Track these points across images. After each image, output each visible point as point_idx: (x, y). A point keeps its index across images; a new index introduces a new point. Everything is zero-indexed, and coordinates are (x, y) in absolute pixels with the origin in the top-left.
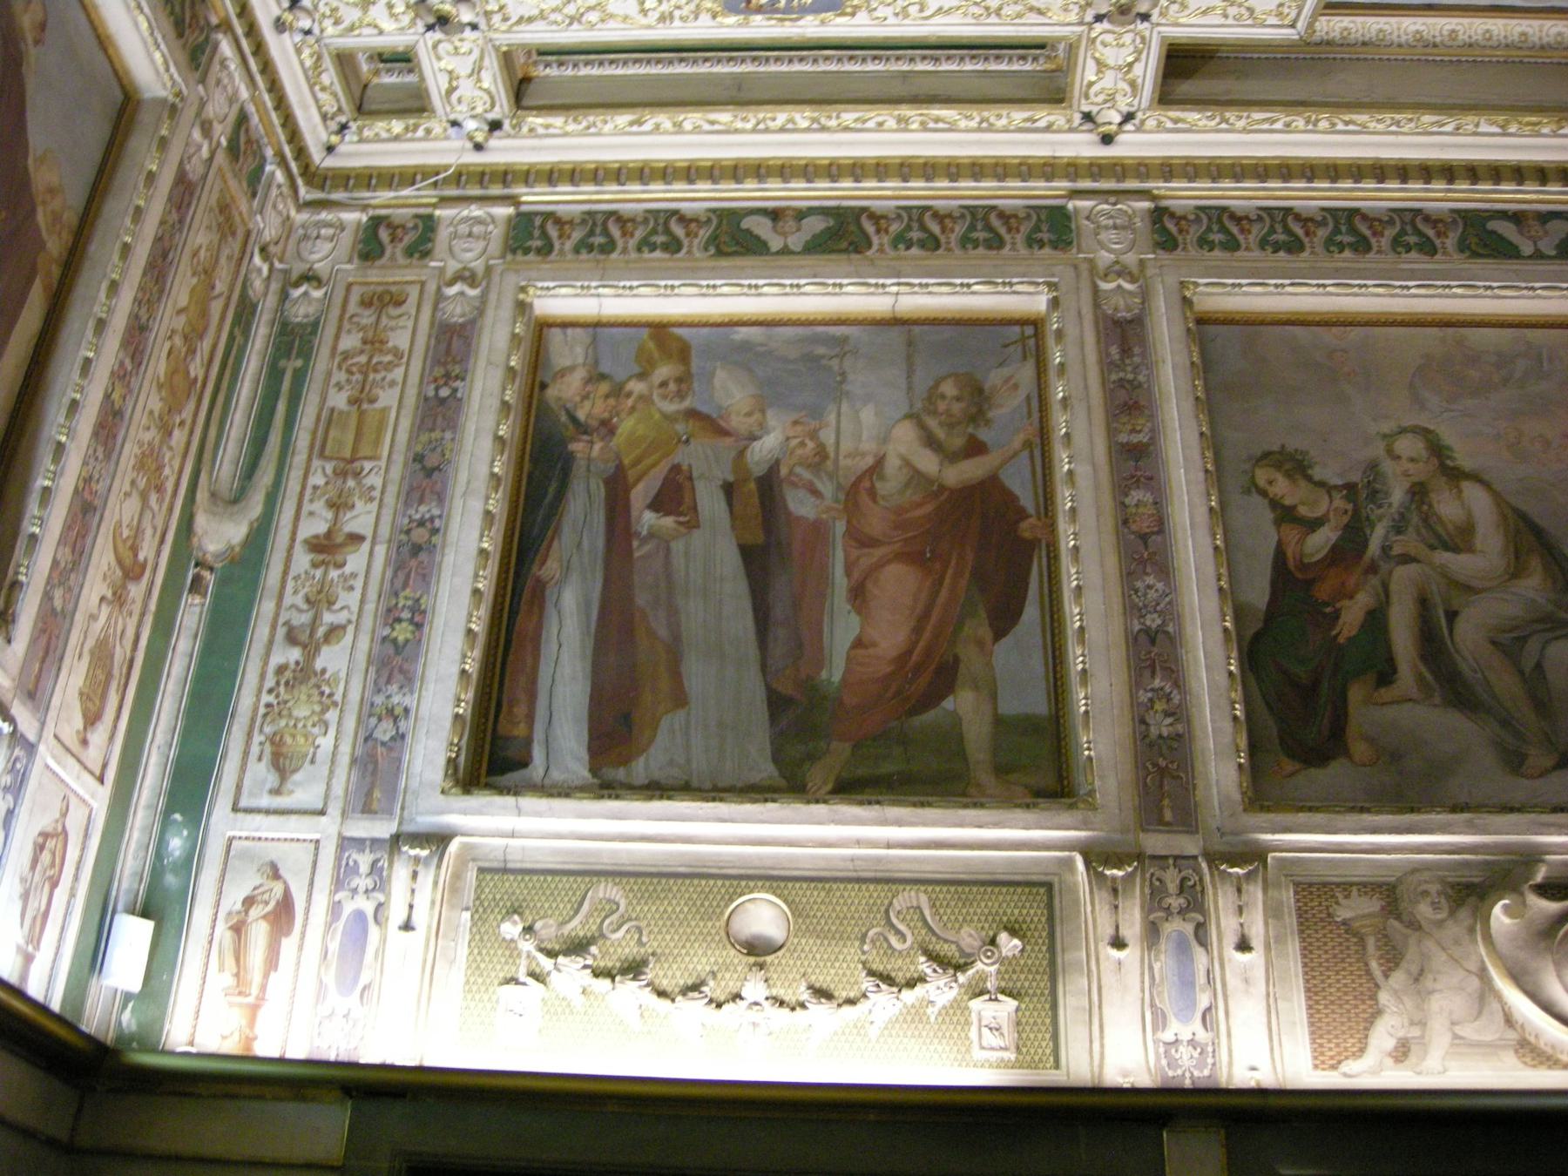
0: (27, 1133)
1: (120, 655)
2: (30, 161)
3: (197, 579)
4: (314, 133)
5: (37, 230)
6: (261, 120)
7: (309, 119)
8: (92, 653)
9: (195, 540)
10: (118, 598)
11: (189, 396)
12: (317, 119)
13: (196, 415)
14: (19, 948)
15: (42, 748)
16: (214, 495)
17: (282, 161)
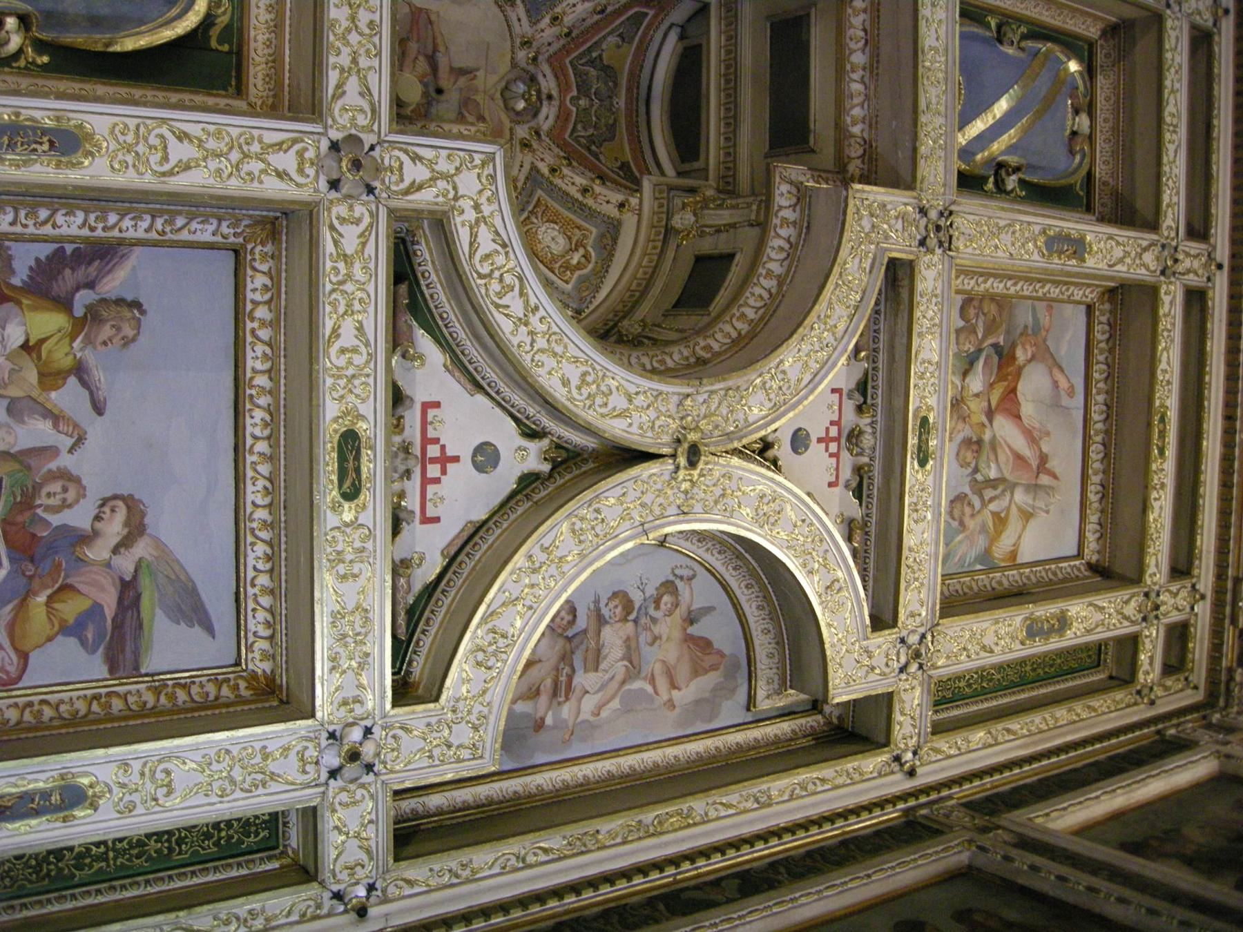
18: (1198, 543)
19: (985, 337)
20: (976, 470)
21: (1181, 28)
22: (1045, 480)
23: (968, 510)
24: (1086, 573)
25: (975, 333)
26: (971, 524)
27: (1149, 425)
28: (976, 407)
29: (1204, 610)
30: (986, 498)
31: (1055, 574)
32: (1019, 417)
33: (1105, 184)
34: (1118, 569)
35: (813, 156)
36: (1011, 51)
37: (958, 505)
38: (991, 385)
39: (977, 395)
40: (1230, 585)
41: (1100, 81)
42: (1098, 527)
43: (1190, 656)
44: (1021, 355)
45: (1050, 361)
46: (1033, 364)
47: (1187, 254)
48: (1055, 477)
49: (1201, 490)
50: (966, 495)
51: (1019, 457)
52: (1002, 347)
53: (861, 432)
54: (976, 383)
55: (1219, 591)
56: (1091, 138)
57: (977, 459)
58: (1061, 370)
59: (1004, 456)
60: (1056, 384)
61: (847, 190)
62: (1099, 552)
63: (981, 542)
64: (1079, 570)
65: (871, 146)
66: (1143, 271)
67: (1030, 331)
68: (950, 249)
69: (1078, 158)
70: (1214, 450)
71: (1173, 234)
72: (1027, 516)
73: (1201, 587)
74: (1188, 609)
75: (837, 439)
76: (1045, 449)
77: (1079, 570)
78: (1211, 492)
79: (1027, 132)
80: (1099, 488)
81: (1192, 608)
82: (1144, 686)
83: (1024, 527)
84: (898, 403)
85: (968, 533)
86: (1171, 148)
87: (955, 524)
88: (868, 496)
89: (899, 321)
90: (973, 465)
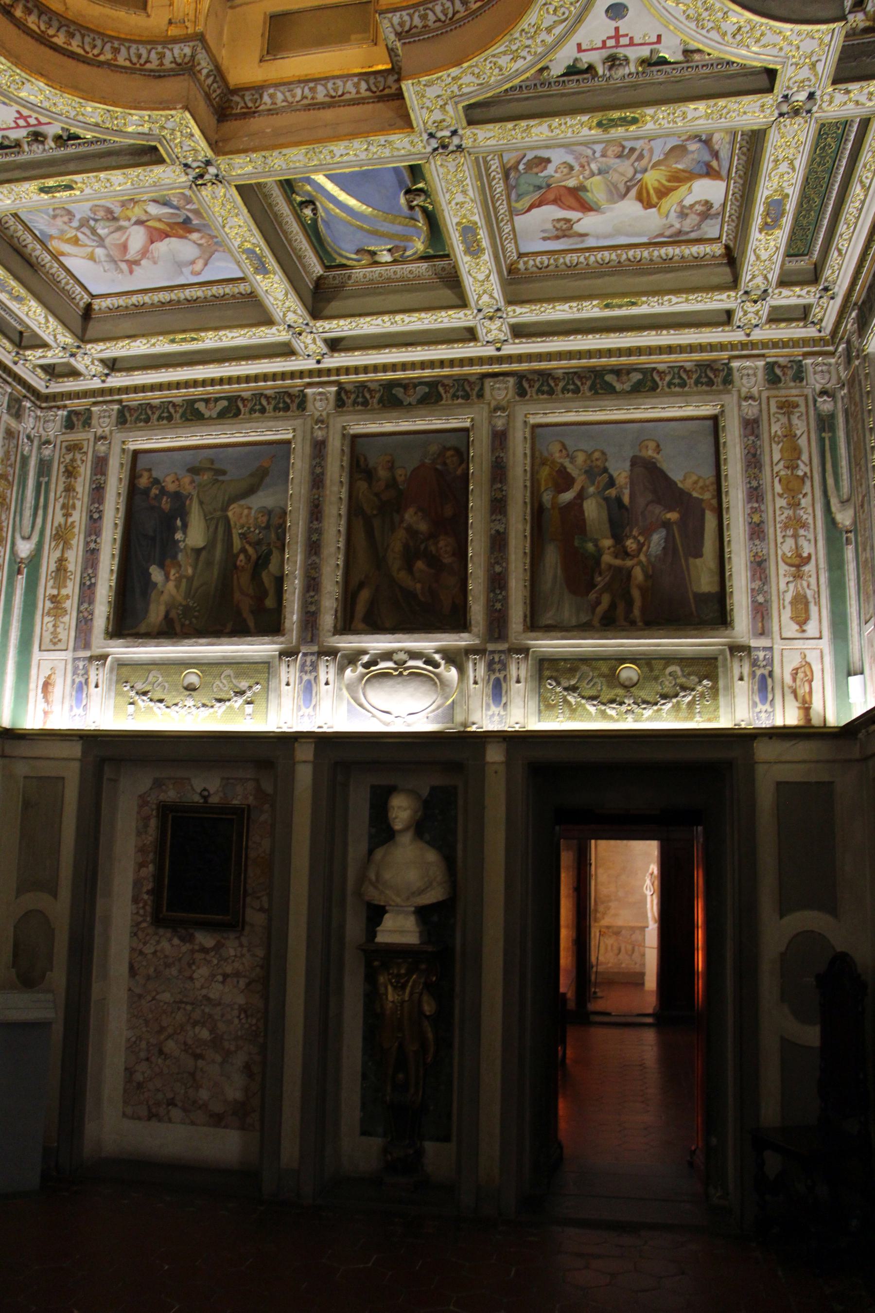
0: (834, 761)
1: (809, 594)
2: (680, 485)
3: (847, 538)
4: (811, 332)
5: (698, 498)
6: (782, 356)
7: (800, 333)
8: (791, 603)
9: (840, 526)
10: (798, 576)
11: (803, 482)
12: (804, 330)
13: (812, 486)
14: (799, 708)
15: (775, 647)
16: (842, 502)
17: (806, 355)
18: (136, 373)
19: (189, 210)
20: (96, 220)
21: (469, 321)
22: (124, 266)
23: (66, 219)
24: (82, 304)
25: (188, 204)
26: (59, 222)
27: (184, 331)
28: (137, 212)
29: (96, 384)
30: (82, 230)
31: (67, 284)
32: (152, 242)
33: (350, 277)
34: (92, 325)
35: (257, 59)
36: (402, 200)
37: (63, 212)
38: (160, 220)
39: (146, 212)
40: (116, 397)
41: (424, 265)
42: (116, 306)
43: (66, 379)
44: (195, 236)
45: (206, 257)
46: (195, 246)
47: (314, 340)
48: (131, 272)
49: (171, 370)
50: (74, 216)
51: (124, 247)
52: (191, 223)
53: (42, 143)
54: (154, 210)
55: (111, 391)
56: (376, 263)
57: (102, 219)
58: (206, 264)
59: (117, 238)
60: (193, 263)
61: (181, 108)
62: (100, 309)
63: (53, 232)
64: (82, 299)
65: (255, 112)
66: (281, 314)
67: (215, 240)
68: (197, 185)
69: (354, 256)
70: (199, 374)
71: (321, 330)
72: (92, 257)
73: (109, 379)
74: (93, 373)
75: (29, 125)
76: (143, 262)
77: (82, 299)
78: (163, 377)
79: (341, 220)
80: (141, 303)
81: (94, 376)
82: (24, 355)
83: (84, 258)
84: (72, 167)
85: (52, 221)
86: (379, 321)
87: (51, 213)
88: (6, 154)
89: (127, 158)
90: (96, 217)
